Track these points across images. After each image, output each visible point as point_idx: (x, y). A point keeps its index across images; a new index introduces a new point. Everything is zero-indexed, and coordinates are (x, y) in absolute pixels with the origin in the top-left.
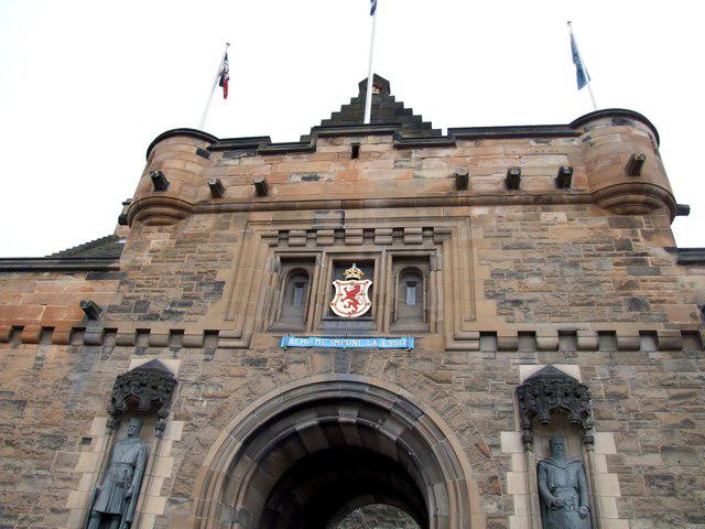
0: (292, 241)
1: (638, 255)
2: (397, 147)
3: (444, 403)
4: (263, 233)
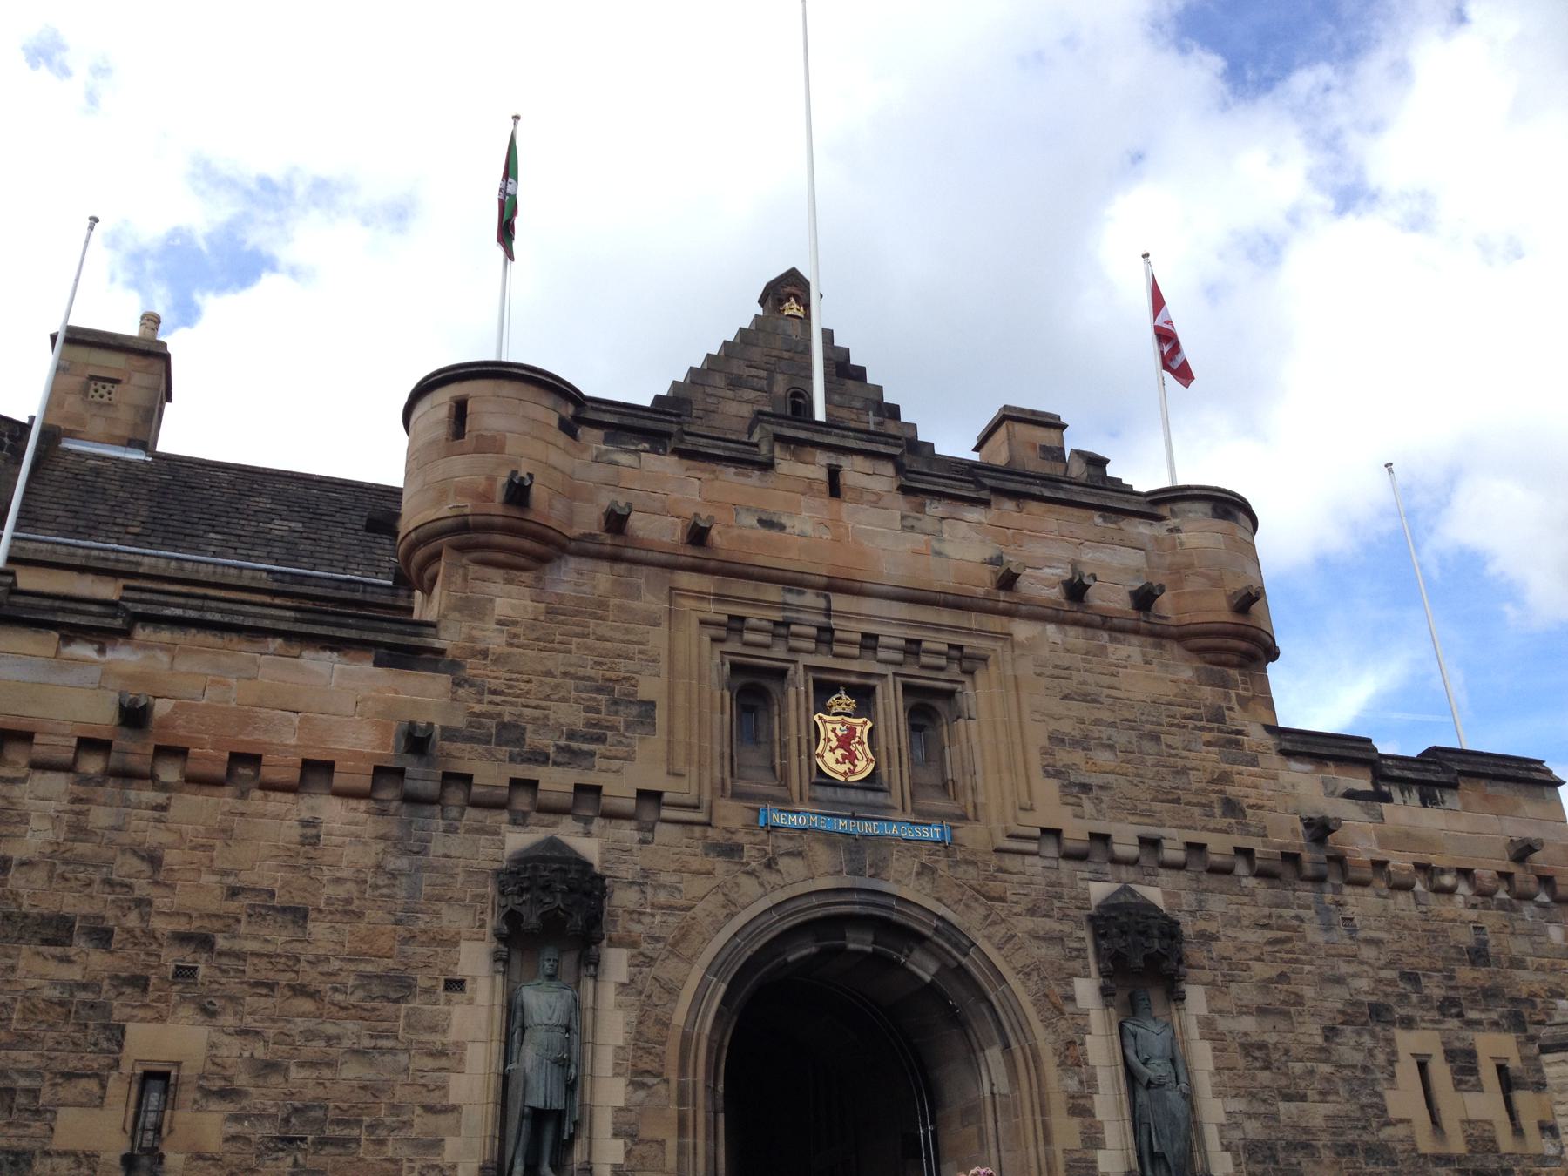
0: (749, 636)
1: (1232, 732)
2: (905, 490)
3: (1000, 931)
4: (703, 616)
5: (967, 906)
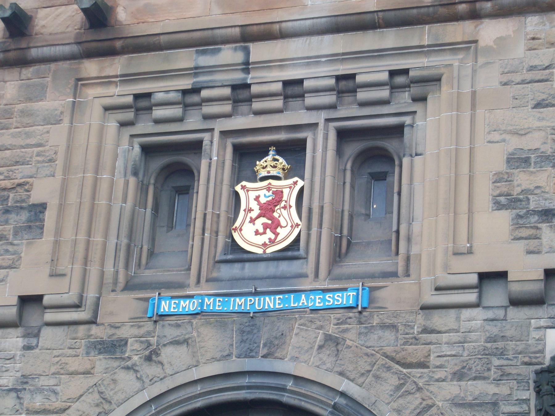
0: (159, 113)
5: (377, 377)
